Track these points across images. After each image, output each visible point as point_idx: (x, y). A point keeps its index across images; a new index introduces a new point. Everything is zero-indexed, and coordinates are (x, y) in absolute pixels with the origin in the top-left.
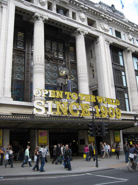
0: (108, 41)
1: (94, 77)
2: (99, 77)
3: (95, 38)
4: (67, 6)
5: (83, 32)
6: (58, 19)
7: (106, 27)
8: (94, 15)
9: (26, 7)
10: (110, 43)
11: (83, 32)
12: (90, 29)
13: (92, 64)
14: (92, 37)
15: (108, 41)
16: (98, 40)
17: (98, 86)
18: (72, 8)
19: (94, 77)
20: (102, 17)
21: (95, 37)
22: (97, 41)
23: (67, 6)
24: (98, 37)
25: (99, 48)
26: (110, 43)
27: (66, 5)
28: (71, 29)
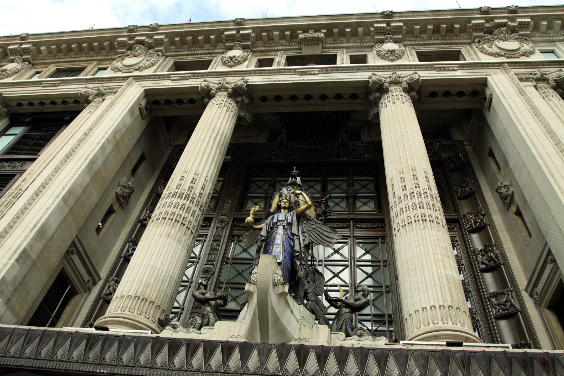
0: (538, 80)
1: (530, 235)
2: (538, 210)
3: (475, 93)
4: (326, 48)
5: (396, 82)
6: (285, 79)
7: (512, 45)
8: (444, 38)
9: (177, 84)
10: (555, 80)
11: (396, 82)
12: (435, 69)
13: (503, 190)
14: (461, 94)
15: (538, 80)
16: (488, 92)
17: (555, 261)
18: (347, 48)
19: (530, 235)
20: (477, 28)
21: (471, 89)
22: (485, 99)
23: (326, 48)
24: (484, 83)
25: (500, 113)
26: (555, 80)
27: (321, 46)
28: (354, 96)
